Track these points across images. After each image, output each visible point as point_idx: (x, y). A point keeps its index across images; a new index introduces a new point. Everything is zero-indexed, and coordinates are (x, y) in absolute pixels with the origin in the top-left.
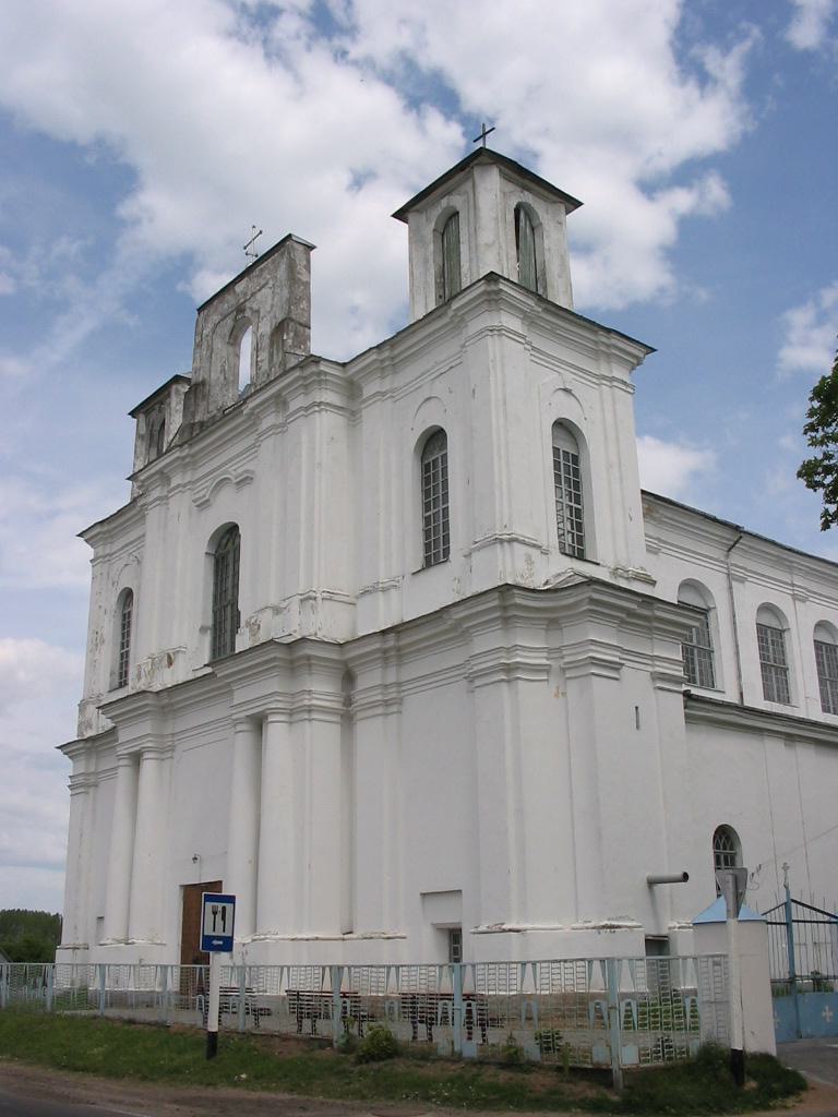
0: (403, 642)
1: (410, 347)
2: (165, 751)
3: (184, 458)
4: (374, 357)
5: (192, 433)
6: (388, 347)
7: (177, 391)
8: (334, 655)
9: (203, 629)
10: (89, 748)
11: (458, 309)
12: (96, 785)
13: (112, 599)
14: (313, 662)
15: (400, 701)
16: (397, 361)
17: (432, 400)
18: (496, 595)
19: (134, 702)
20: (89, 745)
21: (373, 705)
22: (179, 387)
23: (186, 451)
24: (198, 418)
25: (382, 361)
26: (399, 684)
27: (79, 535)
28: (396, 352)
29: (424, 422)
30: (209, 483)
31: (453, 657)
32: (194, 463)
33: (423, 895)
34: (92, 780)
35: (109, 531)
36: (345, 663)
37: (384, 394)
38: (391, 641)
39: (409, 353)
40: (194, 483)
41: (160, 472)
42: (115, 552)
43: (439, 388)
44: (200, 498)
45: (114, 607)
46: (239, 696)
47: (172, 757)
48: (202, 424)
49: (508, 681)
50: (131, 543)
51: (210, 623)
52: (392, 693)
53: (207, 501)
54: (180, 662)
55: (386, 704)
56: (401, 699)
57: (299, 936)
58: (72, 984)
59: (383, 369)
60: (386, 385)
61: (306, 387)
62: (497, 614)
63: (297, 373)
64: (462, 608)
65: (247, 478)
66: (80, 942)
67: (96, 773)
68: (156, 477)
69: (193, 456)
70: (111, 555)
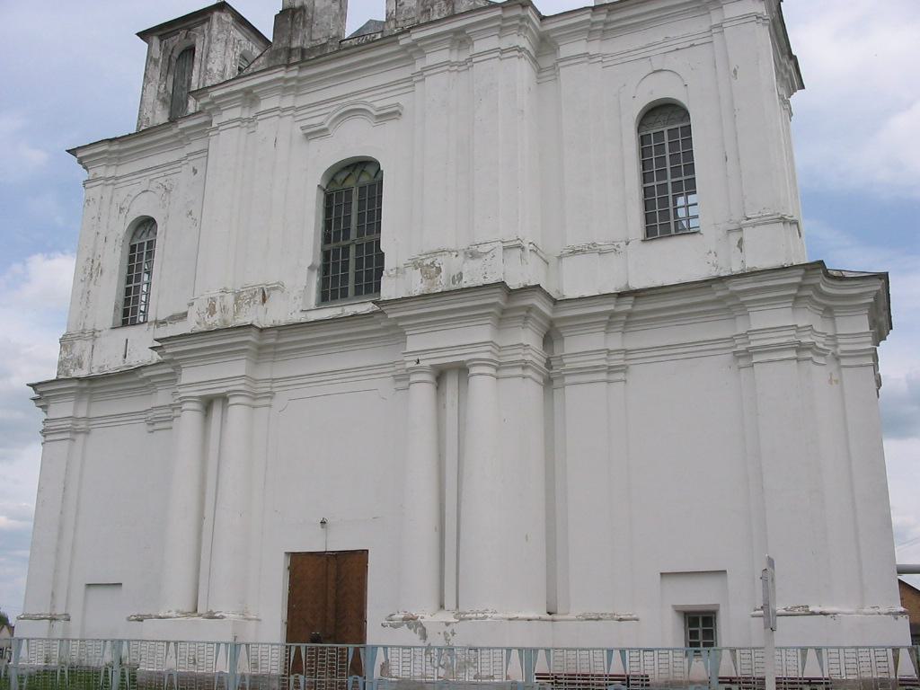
0: (639, 308)
1: (630, 18)
3: (287, 80)
4: (588, 17)
5: (289, 58)
6: (606, 11)
7: (219, 19)
8: (545, 308)
9: (311, 268)
10: (82, 389)
12: (87, 432)
13: (120, 227)
14: (533, 315)
16: (609, 27)
17: (662, 74)
18: (802, 272)
19: (234, 336)
20: (85, 385)
21: (596, 370)
22: (223, 16)
23: (295, 74)
24: (296, 44)
25: (593, 24)
26: (627, 352)
27: (68, 151)
28: (614, 17)
29: (651, 93)
30: (335, 110)
31: (719, 329)
33: (661, 574)
34: (82, 425)
35: (120, 152)
36: (552, 322)
37: (591, 57)
38: (626, 305)
39: (630, 22)
40: (297, 109)
41: (248, 92)
42: (121, 177)
43: (674, 62)
44: (314, 126)
45: (121, 236)
46: (415, 342)
47: (270, 406)
48: (303, 51)
49: (798, 360)
50: (157, 167)
51: (319, 262)
52: (617, 360)
53: (325, 130)
54: (274, 298)
56: (627, 367)
57: (520, 615)
58: (47, 660)
60: (595, 47)
61: (502, 29)
62: (794, 292)
63: (498, 12)
64: (750, 279)
65: (395, 112)
66: (60, 611)
67: (87, 419)
69: (300, 80)
70: (117, 178)
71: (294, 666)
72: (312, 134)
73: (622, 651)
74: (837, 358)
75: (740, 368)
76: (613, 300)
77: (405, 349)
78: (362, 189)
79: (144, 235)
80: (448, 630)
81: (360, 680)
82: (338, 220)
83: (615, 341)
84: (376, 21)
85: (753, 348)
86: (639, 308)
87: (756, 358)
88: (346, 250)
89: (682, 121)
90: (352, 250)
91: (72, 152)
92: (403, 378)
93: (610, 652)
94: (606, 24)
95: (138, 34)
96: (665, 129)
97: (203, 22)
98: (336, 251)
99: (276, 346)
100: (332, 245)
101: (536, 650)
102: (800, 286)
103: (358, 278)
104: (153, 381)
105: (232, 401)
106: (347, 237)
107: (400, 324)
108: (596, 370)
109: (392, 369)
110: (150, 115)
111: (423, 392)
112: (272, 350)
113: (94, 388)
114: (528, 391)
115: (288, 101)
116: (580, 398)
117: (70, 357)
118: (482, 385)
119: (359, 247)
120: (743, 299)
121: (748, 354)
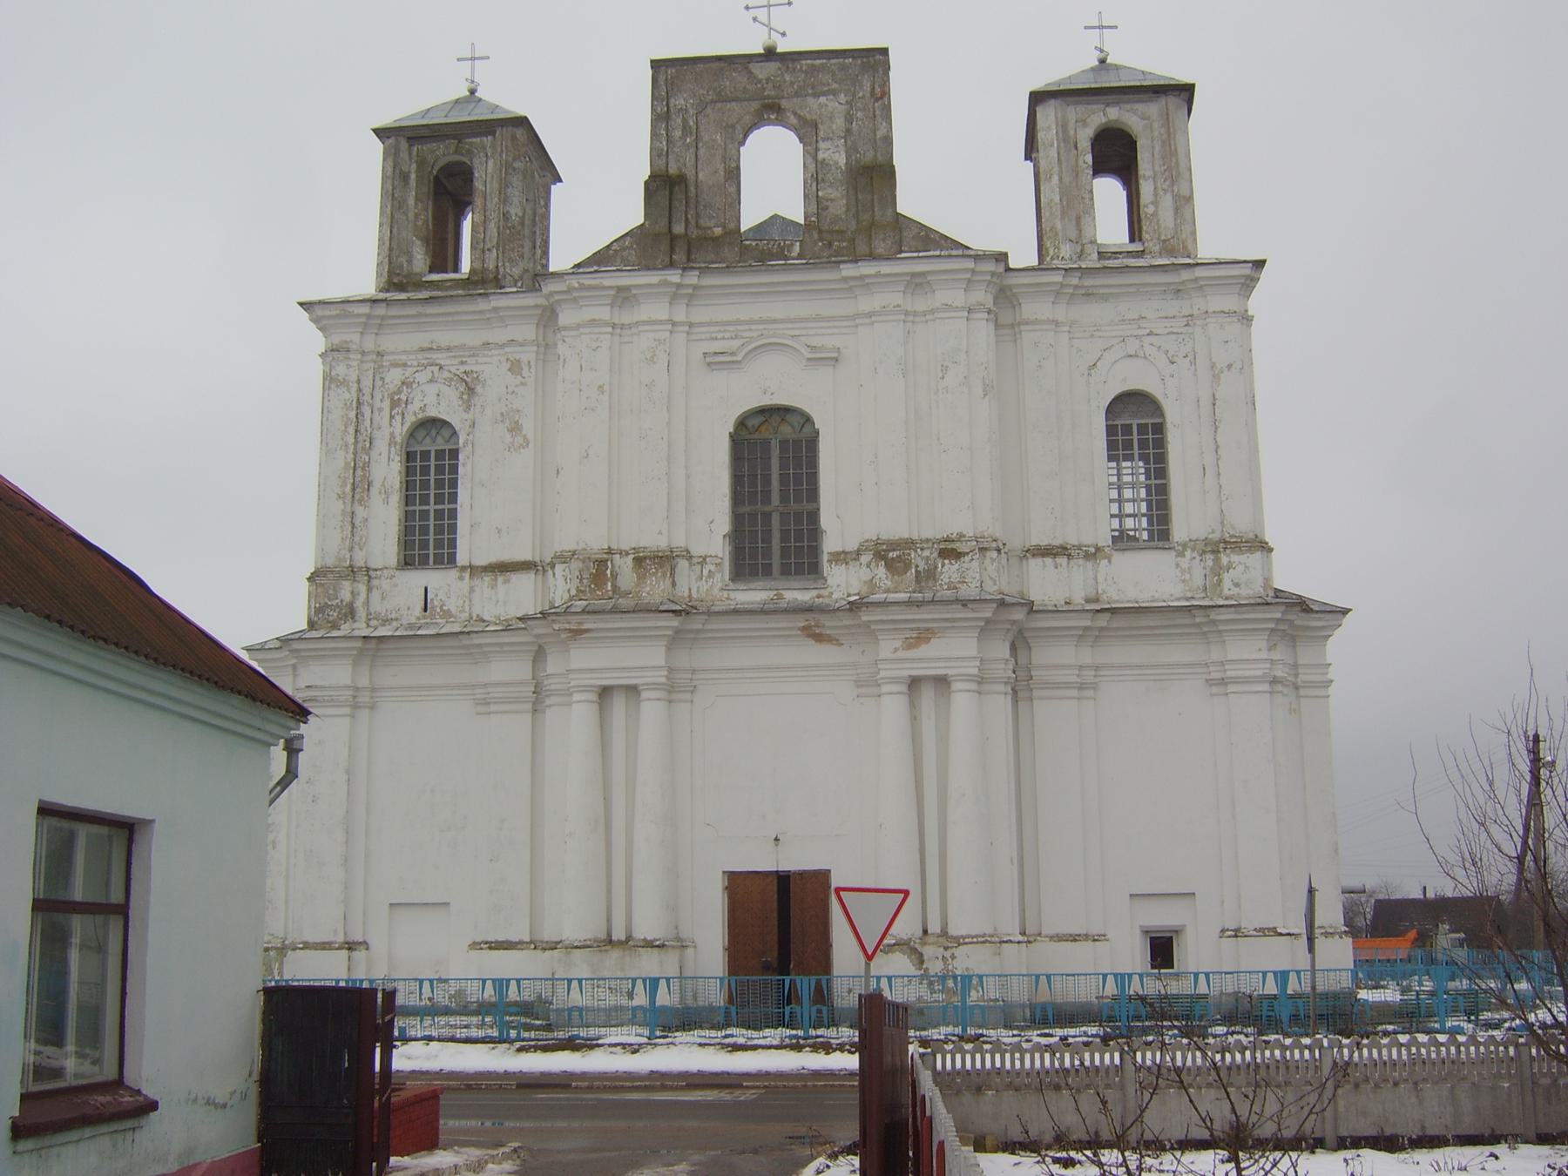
2: (675, 688)
15: (1094, 687)
21: (1067, 686)
25: (1062, 286)
26: (1097, 668)
27: (301, 304)
29: (1125, 380)
32: (691, 296)
33: (1131, 895)
37: (1057, 323)
38: (1103, 620)
46: (888, 646)
53: (739, 362)
55: (1081, 687)
59: (1058, 293)
60: (1061, 312)
63: (970, 264)
68: (613, 292)
69: (695, 287)
72: (716, 362)
73: (1207, 975)
74: (1297, 688)
75: (1212, 695)
76: (1089, 615)
78: (784, 444)
79: (428, 440)
80: (948, 954)
81: (824, 1009)
82: (753, 476)
83: (1086, 656)
84: (784, 218)
85: (1227, 678)
86: (1114, 625)
87: (1231, 688)
88: (767, 517)
89: (1152, 416)
90: (776, 520)
92: (868, 684)
93: (1196, 975)
94: (1076, 287)
95: (374, 130)
96: (1135, 423)
97: (486, 134)
98: (753, 516)
99: (698, 631)
100: (746, 509)
102: (1278, 621)
103: (785, 552)
104: (485, 649)
105: (644, 695)
106: (767, 499)
107: (873, 627)
108: (1067, 686)
109: (854, 672)
110: (403, 259)
112: (692, 636)
114: (1000, 704)
115: (680, 314)
117: (334, 603)
118: (962, 702)
119: (784, 517)
120: (1221, 628)
121: (1223, 682)
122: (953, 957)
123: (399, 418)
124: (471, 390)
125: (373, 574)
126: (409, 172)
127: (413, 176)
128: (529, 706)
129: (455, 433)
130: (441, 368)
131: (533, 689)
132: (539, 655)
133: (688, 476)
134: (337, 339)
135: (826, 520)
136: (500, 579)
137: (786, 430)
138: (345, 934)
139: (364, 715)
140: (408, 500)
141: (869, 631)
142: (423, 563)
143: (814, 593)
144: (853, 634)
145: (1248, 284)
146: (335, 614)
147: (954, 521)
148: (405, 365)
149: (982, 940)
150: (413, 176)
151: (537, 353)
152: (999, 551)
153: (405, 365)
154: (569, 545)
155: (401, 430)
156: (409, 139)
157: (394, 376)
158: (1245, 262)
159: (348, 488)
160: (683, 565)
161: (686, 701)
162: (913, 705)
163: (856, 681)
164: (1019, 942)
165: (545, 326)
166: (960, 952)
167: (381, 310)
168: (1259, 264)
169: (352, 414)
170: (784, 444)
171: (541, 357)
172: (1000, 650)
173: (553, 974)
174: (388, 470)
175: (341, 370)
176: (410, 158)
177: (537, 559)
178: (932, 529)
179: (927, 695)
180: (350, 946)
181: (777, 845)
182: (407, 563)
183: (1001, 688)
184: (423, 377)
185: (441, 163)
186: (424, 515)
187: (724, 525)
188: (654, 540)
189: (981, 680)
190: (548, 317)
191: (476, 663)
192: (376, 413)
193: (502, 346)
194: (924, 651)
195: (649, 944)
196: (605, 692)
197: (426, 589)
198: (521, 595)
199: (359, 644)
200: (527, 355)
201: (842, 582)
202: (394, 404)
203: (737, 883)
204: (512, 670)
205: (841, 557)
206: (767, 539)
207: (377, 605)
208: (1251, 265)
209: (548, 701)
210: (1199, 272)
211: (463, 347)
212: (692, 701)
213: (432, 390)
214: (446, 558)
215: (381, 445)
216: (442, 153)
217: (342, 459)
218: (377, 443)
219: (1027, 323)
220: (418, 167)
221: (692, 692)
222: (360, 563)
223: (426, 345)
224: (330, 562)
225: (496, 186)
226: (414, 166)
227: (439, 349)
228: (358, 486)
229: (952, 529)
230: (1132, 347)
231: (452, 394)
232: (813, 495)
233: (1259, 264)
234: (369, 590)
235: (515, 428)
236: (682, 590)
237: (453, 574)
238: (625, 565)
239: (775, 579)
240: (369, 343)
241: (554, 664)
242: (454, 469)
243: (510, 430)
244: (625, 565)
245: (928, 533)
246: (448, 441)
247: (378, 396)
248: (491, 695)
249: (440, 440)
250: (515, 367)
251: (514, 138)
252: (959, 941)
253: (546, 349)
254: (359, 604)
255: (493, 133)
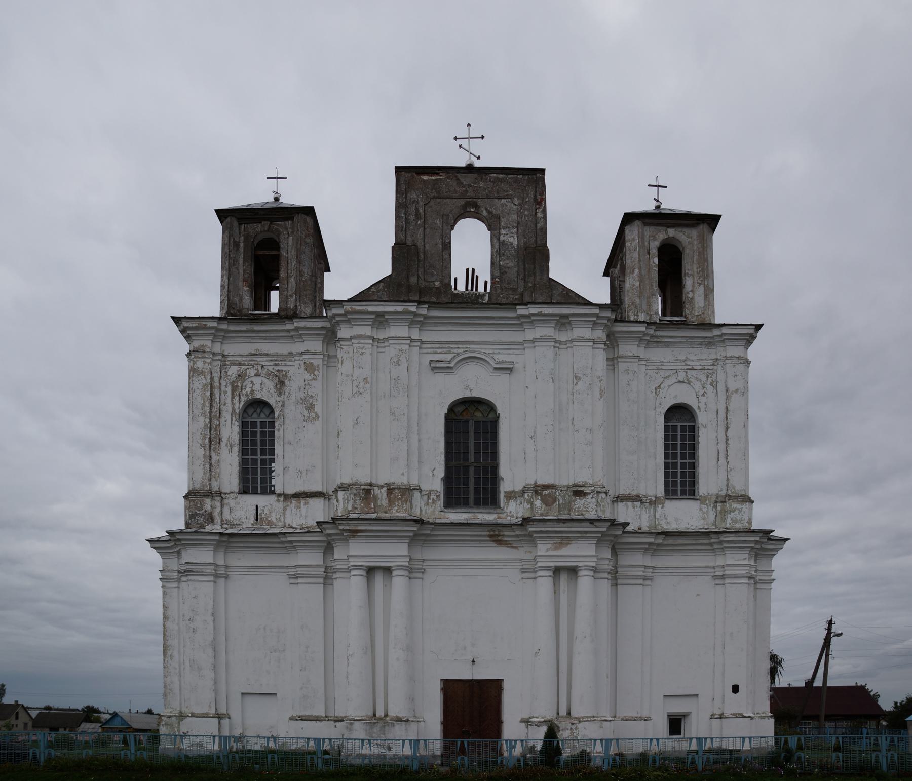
2: (413, 571)
6: (654, 327)
9: (442, 479)
11: (726, 334)
25: (645, 334)
60: (641, 352)
71: (446, 747)
77: (537, 553)
80: (573, 727)
88: (466, 468)
91: (177, 320)
94: (652, 336)
97: (287, 219)
101: (611, 740)
103: (477, 491)
104: (294, 544)
106: (466, 458)
109: (520, 564)
111: (545, 583)
113: (229, 542)
114: (605, 585)
116: (631, 593)
117: (201, 512)
118: (585, 582)
122: (576, 729)
123: (237, 398)
124: (282, 383)
125: (224, 496)
126: (239, 242)
127: (242, 245)
128: (321, 580)
129: (272, 411)
130: (263, 367)
131: (324, 570)
132: (328, 549)
133: (420, 440)
134: (196, 344)
135: (503, 471)
136: (303, 502)
137: (478, 415)
138: (216, 709)
139: (221, 582)
140: (244, 452)
141: (531, 539)
142: (255, 492)
143: (495, 516)
144: (520, 540)
145: (750, 339)
146: (202, 519)
147: (581, 476)
148: (240, 364)
149: (593, 719)
150: (242, 245)
151: (323, 360)
152: (606, 493)
153: (240, 364)
154: (347, 480)
155: (239, 406)
156: (238, 219)
157: (233, 371)
158: (751, 325)
159: (207, 441)
160: (417, 494)
161: (419, 578)
162: (556, 584)
163: (521, 569)
164: (610, 721)
165: (328, 344)
166: (580, 726)
167: (224, 326)
168: (758, 327)
169: (208, 393)
170: (477, 423)
171: (326, 363)
172: (607, 554)
173: (343, 735)
174: (231, 431)
175: (199, 364)
176: (240, 233)
177: (325, 491)
178: (565, 480)
179: (564, 578)
180: (219, 717)
181: (473, 665)
182: (244, 491)
183: (606, 575)
184: (252, 372)
185: (260, 237)
186: (255, 462)
187: (441, 473)
188: (399, 478)
189: (595, 570)
190: (330, 337)
191: (289, 553)
192: (222, 393)
193: (302, 354)
194: (564, 551)
195: (399, 720)
196: (370, 571)
197: (257, 506)
198: (316, 511)
199: (217, 538)
200: (317, 361)
201: (514, 511)
202: (234, 389)
203: (449, 686)
204: (311, 559)
205: (510, 496)
206: (466, 484)
207: (227, 515)
208: (754, 327)
209: (334, 576)
210: (725, 330)
211: (277, 355)
212: (423, 579)
213: (257, 380)
214: (268, 490)
215: (227, 415)
216: (258, 229)
217: (202, 421)
218: (224, 414)
219: (622, 357)
220: (244, 239)
221: (423, 573)
222: (215, 488)
223: (253, 352)
224: (198, 486)
225: (294, 253)
226: (242, 238)
227: (261, 355)
228: (212, 439)
229: (579, 480)
230: (682, 376)
231: (270, 384)
232: (495, 455)
233: (758, 327)
234: (222, 506)
235: (310, 407)
236: (417, 512)
237: (273, 498)
238: (381, 495)
239: (471, 507)
240: (217, 348)
241: (339, 553)
242: (272, 434)
243: (307, 409)
244: (381, 495)
245: (565, 482)
246: (268, 417)
247: (223, 383)
248: (298, 573)
249: (263, 415)
250: (310, 368)
251: (305, 222)
252: (580, 720)
253: (329, 358)
254: (216, 514)
255: (292, 219)
